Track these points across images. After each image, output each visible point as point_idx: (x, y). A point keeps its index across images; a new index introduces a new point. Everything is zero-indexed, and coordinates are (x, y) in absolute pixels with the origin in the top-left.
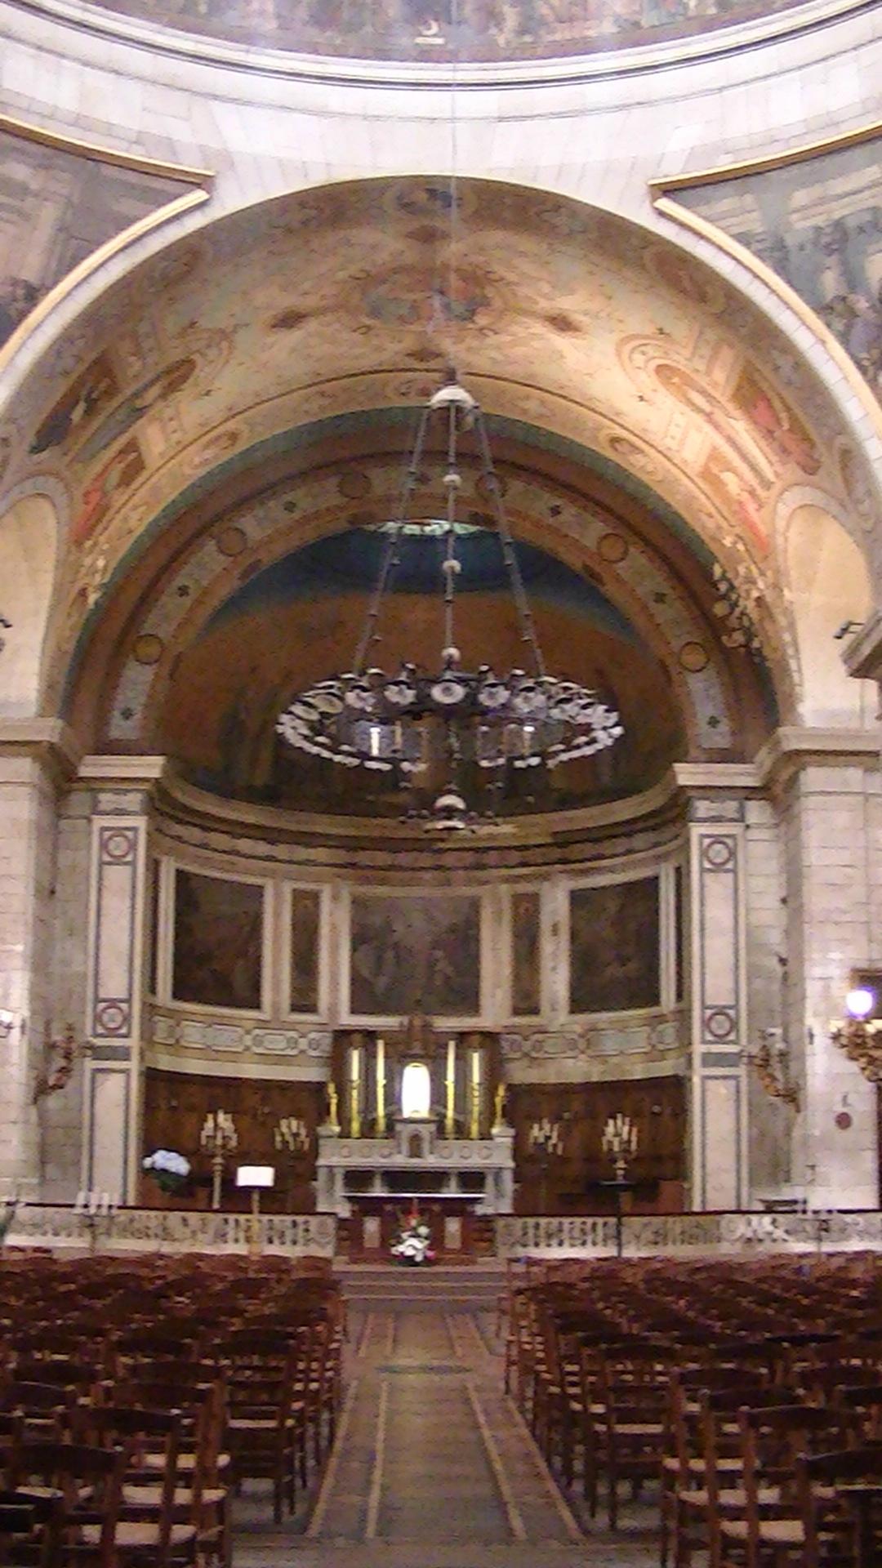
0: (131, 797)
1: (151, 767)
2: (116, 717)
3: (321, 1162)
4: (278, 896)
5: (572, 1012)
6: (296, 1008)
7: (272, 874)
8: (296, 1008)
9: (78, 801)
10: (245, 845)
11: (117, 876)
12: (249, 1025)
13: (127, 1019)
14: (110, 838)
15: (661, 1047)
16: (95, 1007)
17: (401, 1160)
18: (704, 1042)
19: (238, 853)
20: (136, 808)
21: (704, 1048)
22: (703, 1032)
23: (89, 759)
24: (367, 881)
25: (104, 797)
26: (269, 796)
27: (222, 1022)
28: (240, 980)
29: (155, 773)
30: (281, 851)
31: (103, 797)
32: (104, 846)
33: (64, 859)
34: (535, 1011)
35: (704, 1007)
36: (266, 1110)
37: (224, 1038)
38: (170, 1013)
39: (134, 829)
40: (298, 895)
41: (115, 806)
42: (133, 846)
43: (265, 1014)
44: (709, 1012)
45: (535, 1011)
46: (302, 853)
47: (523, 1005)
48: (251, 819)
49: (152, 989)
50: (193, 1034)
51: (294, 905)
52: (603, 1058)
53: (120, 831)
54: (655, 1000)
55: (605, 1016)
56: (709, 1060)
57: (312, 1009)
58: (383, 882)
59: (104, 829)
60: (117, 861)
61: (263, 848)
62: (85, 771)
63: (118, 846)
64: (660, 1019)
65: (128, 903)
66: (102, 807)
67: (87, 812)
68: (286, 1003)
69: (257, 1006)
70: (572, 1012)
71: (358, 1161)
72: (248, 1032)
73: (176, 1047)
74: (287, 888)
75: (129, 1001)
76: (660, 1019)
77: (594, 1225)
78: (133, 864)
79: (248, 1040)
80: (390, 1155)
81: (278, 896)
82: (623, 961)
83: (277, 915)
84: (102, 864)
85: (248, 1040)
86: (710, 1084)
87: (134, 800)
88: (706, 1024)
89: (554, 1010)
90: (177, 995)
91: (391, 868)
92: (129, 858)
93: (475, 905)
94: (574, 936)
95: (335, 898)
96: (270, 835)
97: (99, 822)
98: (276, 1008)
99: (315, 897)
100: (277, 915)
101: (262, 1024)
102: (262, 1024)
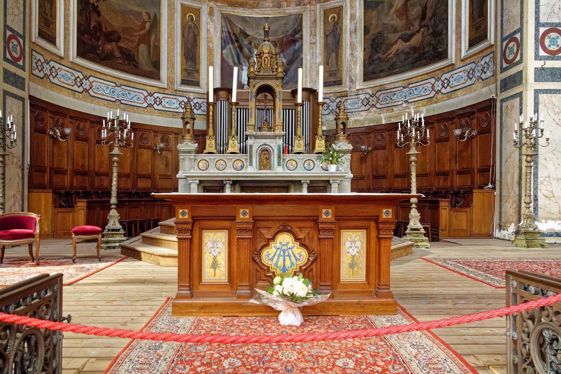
3: (180, 175)
5: (365, 80)
6: (184, 82)
8: (184, 82)
12: (151, 90)
15: (449, 89)
18: (537, 57)
21: (539, 64)
22: (537, 49)
34: (339, 83)
35: (538, 24)
36: (162, 145)
38: (74, 67)
43: (164, 83)
44: (542, 30)
45: (339, 83)
47: (332, 79)
51: (183, 15)
52: (390, 108)
54: (443, 55)
55: (392, 79)
56: (541, 75)
57: (197, 84)
64: (452, 67)
68: (178, 79)
69: (157, 77)
70: (365, 80)
71: (213, 172)
72: (151, 95)
76: (452, 67)
79: (151, 100)
80: (242, 167)
82: (406, 39)
85: (151, 100)
86: (543, 97)
88: (540, 41)
89: (352, 81)
90: (81, 53)
93: (299, 19)
94: (367, 30)
95: (211, 14)
98: (171, 81)
99: (197, 12)
100: (171, 18)
101: (162, 90)
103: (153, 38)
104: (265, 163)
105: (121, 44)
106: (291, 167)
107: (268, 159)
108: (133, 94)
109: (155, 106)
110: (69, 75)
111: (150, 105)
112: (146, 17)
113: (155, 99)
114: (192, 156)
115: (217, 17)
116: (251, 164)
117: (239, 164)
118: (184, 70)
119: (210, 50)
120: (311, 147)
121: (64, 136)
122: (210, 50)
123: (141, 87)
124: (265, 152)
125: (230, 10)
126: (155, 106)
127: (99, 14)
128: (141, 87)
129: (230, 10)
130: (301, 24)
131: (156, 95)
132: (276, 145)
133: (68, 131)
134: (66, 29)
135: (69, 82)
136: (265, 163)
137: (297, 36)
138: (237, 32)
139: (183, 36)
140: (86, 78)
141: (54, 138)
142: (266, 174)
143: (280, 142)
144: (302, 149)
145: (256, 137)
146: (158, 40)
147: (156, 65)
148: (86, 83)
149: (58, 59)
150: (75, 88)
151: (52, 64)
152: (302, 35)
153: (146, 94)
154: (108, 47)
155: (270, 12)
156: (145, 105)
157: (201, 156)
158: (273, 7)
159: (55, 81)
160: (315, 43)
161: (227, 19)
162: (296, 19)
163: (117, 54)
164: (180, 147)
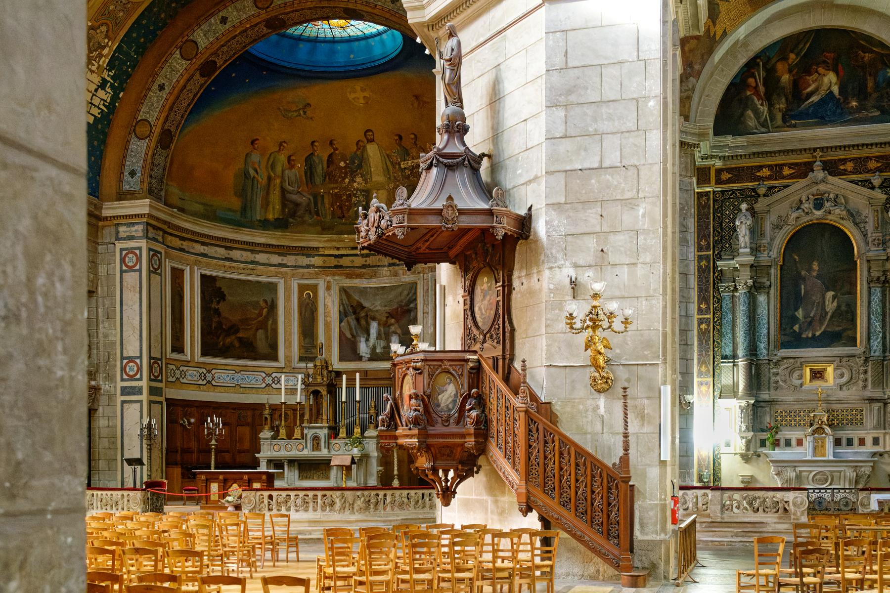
0: (136, 227)
1: (142, 206)
2: (126, 177)
4: (288, 289)
6: (302, 359)
7: (284, 276)
8: (302, 359)
9: (107, 233)
10: (261, 257)
11: (131, 279)
13: (140, 369)
14: (126, 254)
16: (122, 363)
17: (307, 453)
19: (257, 263)
20: (140, 234)
23: (106, 205)
24: (349, 276)
25: (122, 229)
26: (281, 224)
27: (253, 370)
28: (261, 344)
29: (146, 211)
30: (290, 260)
31: (122, 229)
32: (123, 261)
33: (102, 270)
37: (256, 379)
38: (199, 365)
39: (140, 248)
40: (302, 288)
41: (128, 234)
42: (139, 259)
43: (281, 363)
46: (304, 261)
48: (262, 240)
49: (178, 348)
50: (222, 377)
53: (131, 251)
58: (360, 276)
59: (121, 250)
60: (131, 269)
61: (276, 259)
62: (106, 213)
63: (131, 260)
65: (138, 295)
66: (121, 235)
67: (113, 240)
68: (296, 358)
69: (275, 358)
72: (269, 375)
73: (735, 385)
74: (294, 285)
75: (140, 357)
77: (385, 495)
78: (140, 270)
79: (269, 380)
81: (288, 289)
83: (288, 298)
84: (122, 272)
87: (138, 230)
90: (204, 353)
91: (364, 266)
92: (137, 267)
93: (413, 286)
95: (328, 288)
96: (283, 250)
97: (120, 245)
98: (288, 359)
99: (314, 288)
100: (288, 298)
102: (280, 370)
103: (270, 322)
104: (316, 447)
105: (240, 335)
106: (336, 449)
107: (318, 444)
108: (251, 377)
109: (273, 385)
110: (195, 373)
111: (268, 385)
112: (262, 304)
113: (273, 379)
114: (269, 442)
115: (335, 290)
116: (306, 447)
117: (301, 447)
118: (301, 347)
119: (327, 325)
120: (350, 433)
121: (190, 424)
122: (327, 325)
123: (260, 369)
124: (316, 438)
125: (348, 283)
126: (273, 385)
127: (219, 314)
128: (260, 369)
129: (348, 283)
130: (415, 293)
131: (274, 375)
132: (323, 433)
133: (192, 420)
134: (192, 337)
135: (195, 378)
136: (316, 447)
137: (412, 305)
138: (355, 304)
139: (300, 313)
140: (209, 371)
141: (183, 426)
142: (316, 454)
143: (326, 431)
144: (344, 435)
145: (310, 428)
146: (275, 322)
147: (274, 347)
148: (209, 377)
149: (185, 364)
150: (201, 382)
151: (181, 368)
152: (416, 305)
153: (264, 375)
154: (228, 340)
155: (387, 281)
156: (264, 385)
157: (275, 442)
158: (391, 276)
159: (185, 381)
160: (427, 313)
161: (344, 291)
162: (411, 288)
163: (237, 344)
164: (261, 435)
